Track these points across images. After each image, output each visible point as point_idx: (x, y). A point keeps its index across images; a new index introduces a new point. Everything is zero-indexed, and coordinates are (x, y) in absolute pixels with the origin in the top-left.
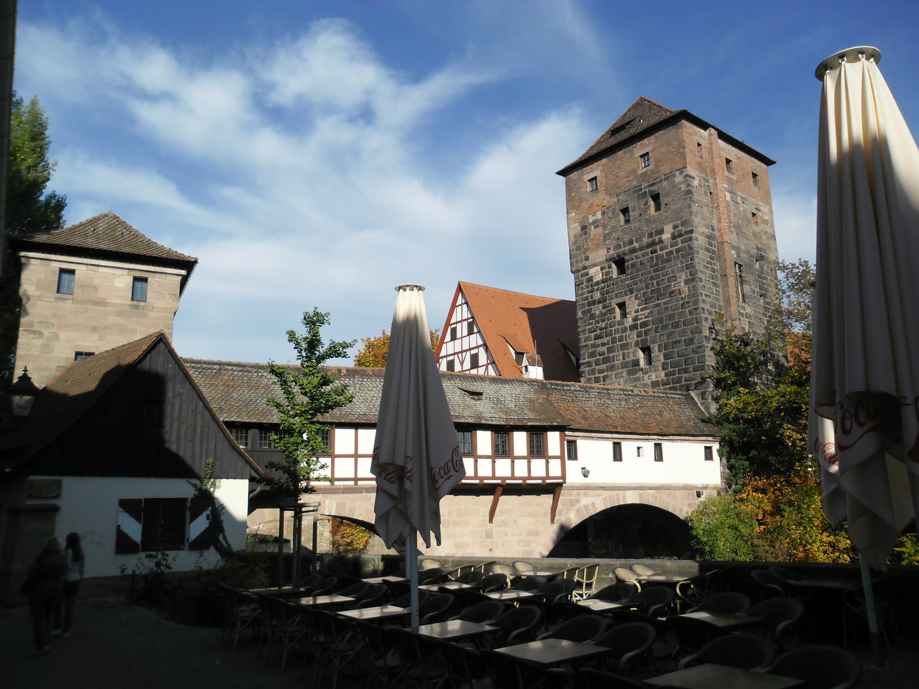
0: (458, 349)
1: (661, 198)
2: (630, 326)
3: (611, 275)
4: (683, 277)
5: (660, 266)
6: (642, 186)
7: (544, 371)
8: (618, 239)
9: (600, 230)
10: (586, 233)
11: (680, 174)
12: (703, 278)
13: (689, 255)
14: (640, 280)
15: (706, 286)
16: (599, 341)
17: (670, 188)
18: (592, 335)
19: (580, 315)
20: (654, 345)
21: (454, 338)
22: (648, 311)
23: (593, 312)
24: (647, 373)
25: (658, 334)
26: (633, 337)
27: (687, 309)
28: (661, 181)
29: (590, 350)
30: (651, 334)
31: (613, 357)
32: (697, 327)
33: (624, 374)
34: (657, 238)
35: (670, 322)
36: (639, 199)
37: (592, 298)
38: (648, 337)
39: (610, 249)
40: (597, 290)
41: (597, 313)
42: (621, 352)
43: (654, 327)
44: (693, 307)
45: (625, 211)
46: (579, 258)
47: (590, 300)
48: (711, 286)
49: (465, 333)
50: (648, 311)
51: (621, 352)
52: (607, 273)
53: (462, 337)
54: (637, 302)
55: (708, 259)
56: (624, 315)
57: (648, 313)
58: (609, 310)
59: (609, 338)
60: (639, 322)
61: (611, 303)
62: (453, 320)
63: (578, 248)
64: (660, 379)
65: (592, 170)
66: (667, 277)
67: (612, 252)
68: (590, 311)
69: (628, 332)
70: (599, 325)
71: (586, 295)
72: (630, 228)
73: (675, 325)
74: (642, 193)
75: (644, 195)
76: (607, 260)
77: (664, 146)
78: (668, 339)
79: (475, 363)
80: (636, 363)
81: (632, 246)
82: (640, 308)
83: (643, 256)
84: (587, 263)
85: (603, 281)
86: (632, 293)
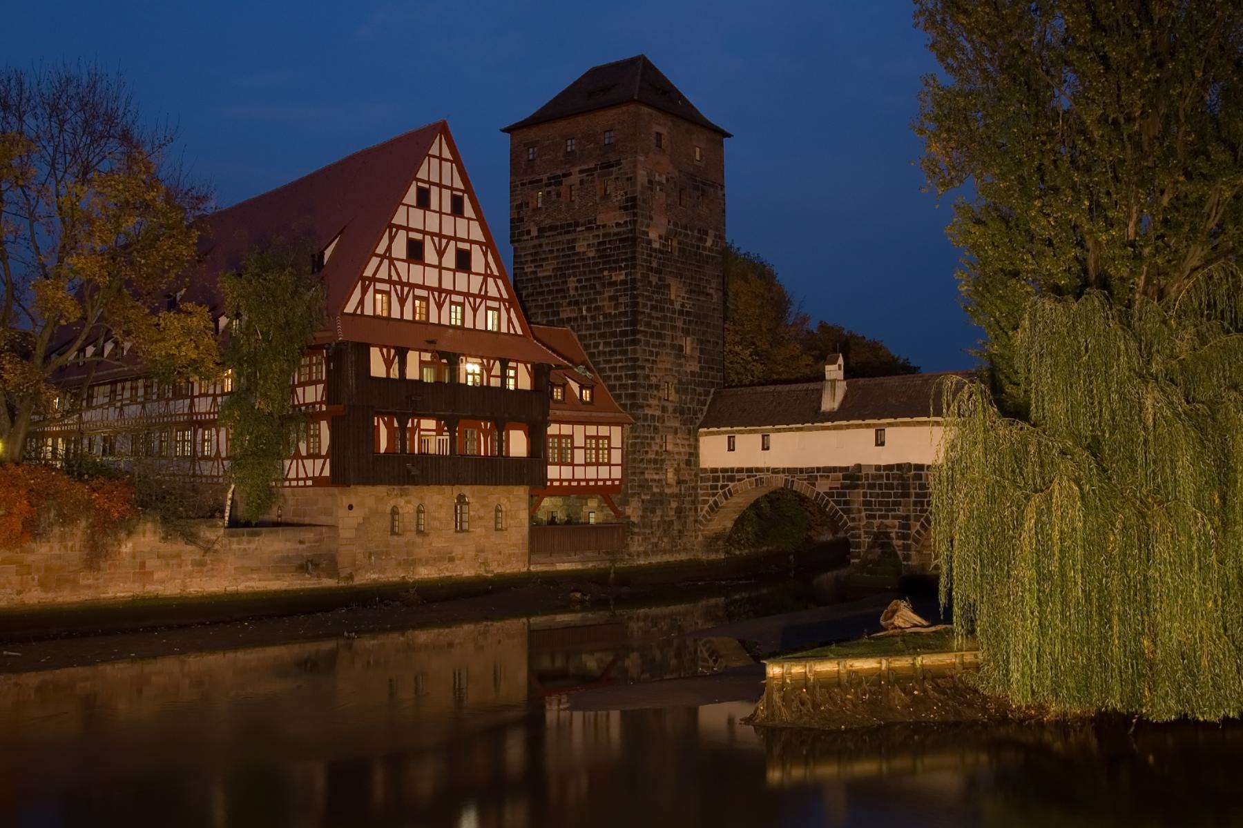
42: (670, 333)
60: (685, 309)
71: (645, 257)
79: (463, 261)
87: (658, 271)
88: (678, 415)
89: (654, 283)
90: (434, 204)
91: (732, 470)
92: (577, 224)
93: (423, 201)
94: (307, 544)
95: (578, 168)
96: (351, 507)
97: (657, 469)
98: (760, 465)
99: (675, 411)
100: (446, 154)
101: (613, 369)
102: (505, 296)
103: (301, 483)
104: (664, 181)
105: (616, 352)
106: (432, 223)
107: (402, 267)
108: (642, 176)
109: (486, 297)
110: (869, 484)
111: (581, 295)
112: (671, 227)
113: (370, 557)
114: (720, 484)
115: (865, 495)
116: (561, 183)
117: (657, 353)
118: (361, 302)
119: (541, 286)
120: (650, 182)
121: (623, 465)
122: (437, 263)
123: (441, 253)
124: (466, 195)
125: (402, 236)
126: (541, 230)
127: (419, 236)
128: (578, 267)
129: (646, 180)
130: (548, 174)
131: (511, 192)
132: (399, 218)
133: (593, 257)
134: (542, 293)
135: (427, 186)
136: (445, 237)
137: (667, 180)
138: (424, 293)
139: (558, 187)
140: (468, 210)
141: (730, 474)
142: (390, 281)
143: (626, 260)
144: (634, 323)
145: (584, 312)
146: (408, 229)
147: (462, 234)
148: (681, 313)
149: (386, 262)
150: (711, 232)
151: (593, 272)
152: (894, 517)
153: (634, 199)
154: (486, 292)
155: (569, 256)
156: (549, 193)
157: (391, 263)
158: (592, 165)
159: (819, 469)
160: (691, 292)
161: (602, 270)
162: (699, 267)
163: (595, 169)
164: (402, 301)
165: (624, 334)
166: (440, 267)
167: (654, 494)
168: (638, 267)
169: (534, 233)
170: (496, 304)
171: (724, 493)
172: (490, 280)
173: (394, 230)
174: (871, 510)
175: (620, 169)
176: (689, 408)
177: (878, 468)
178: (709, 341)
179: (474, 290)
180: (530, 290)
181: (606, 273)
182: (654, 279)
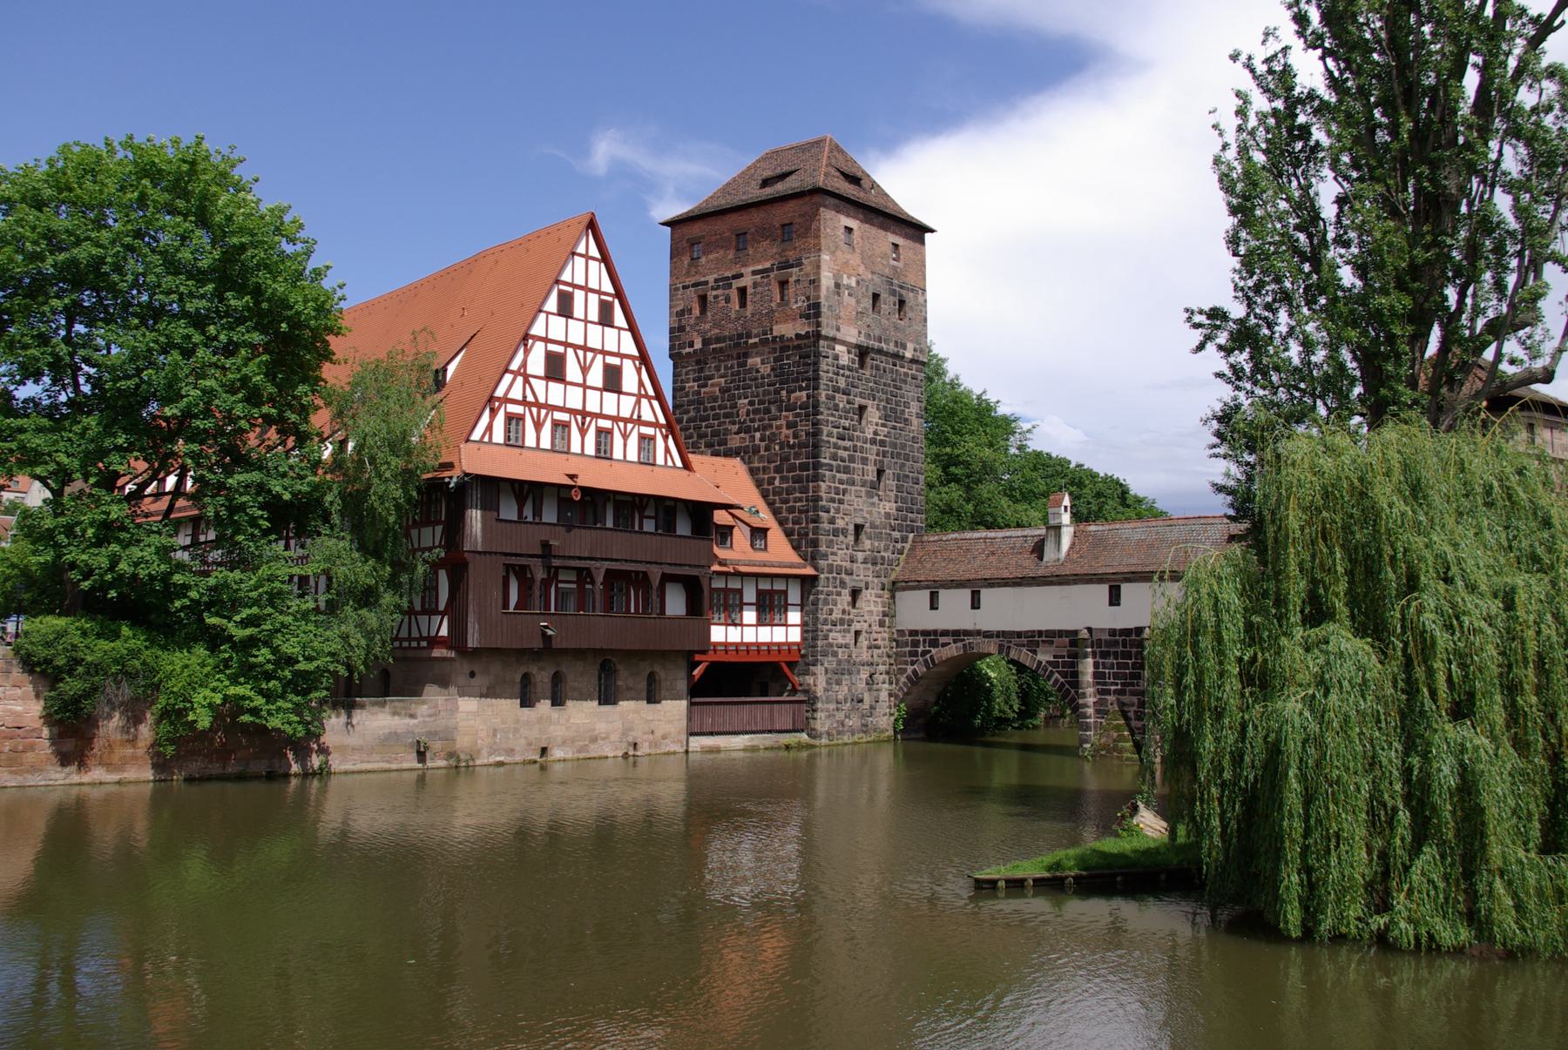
16: (840, 443)
19: (823, 398)
45: (876, 297)
67: (862, 338)
79: (612, 381)
84: (839, 336)
87: (844, 393)
88: (869, 565)
89: (841, 405)
90: (578, 311)
91: (935, 632)
92: (749, 336)
93: (565, 310)
94: (420, 719)
95: (751, 269)
96: (472, 675)
97: (844, 631)
98: (969, 626)
99: (865, 562)
100: (594, 252)
101: (791, 510)
102: (662, 420)
103: (414, 644)
104: (854, 284)
105: (795, 489)
106: (576, 334)
107: (539, 385)
108: (827, 280)
109: (639, 422)
110: (1101, 652)
111: (752, 421)
112: (862, 338)
113: (495, 735)
114: (920, 650)
115: (1096, 665)
116: (730, 286)
117: (845, 491)
118: (489, 428)
119: (705, 410)
120: (837, 286)
121: (804, 625)
122: (581, 381)
123: (585, 370)
124: (616, 302)
125: (539, 347)
126: (706, 342)
127: (560, 349)
128: (750, 387)
129: (832, 283)
130: (716, 276)
131: (671, 296)
132: (538, 329)
133: (769, 375)
134: (706, 419)
135: (570, 289)
136: (591, 350)
137: (858, 283)
138: (564, 417)
139: (727, 292)
140: (619, 318)
141: (933, 637)
142: (524, 402)
143: (808, 379)
144: (816, 456)
145: (757, 442)
146: (546, 340)
147: (611, 346)
148: (873, 442)
149: (520, 379)
150: (910, 346)
151: (769, 393)
152: (1133, 693)
153: (817, 306)
154: (639, 416)
155: (738, 373)
156: (716, 297)
157: (526, 381)
158: (768, 265)
159: (1040, 633)
160: (886, 418)
161: (777, 392)
162: (895, 387)
163: (770, 270)
164: (538, 426)
165: (804, 467)
166: (584, 386)
167: (839, 662)
168: (822, 387)
169: (698, 345)
170: (649, 431)
171: (926, 661)
172: (644, 402)
173: (530, 341)
174: (1105, 684)
175: (801, 270)
176: (883, 558)
177: (1113, 632)
178: (907, 476)
179: (626, 413)
180: (692, 414)
181: (784, 393)
182: (841, 401)
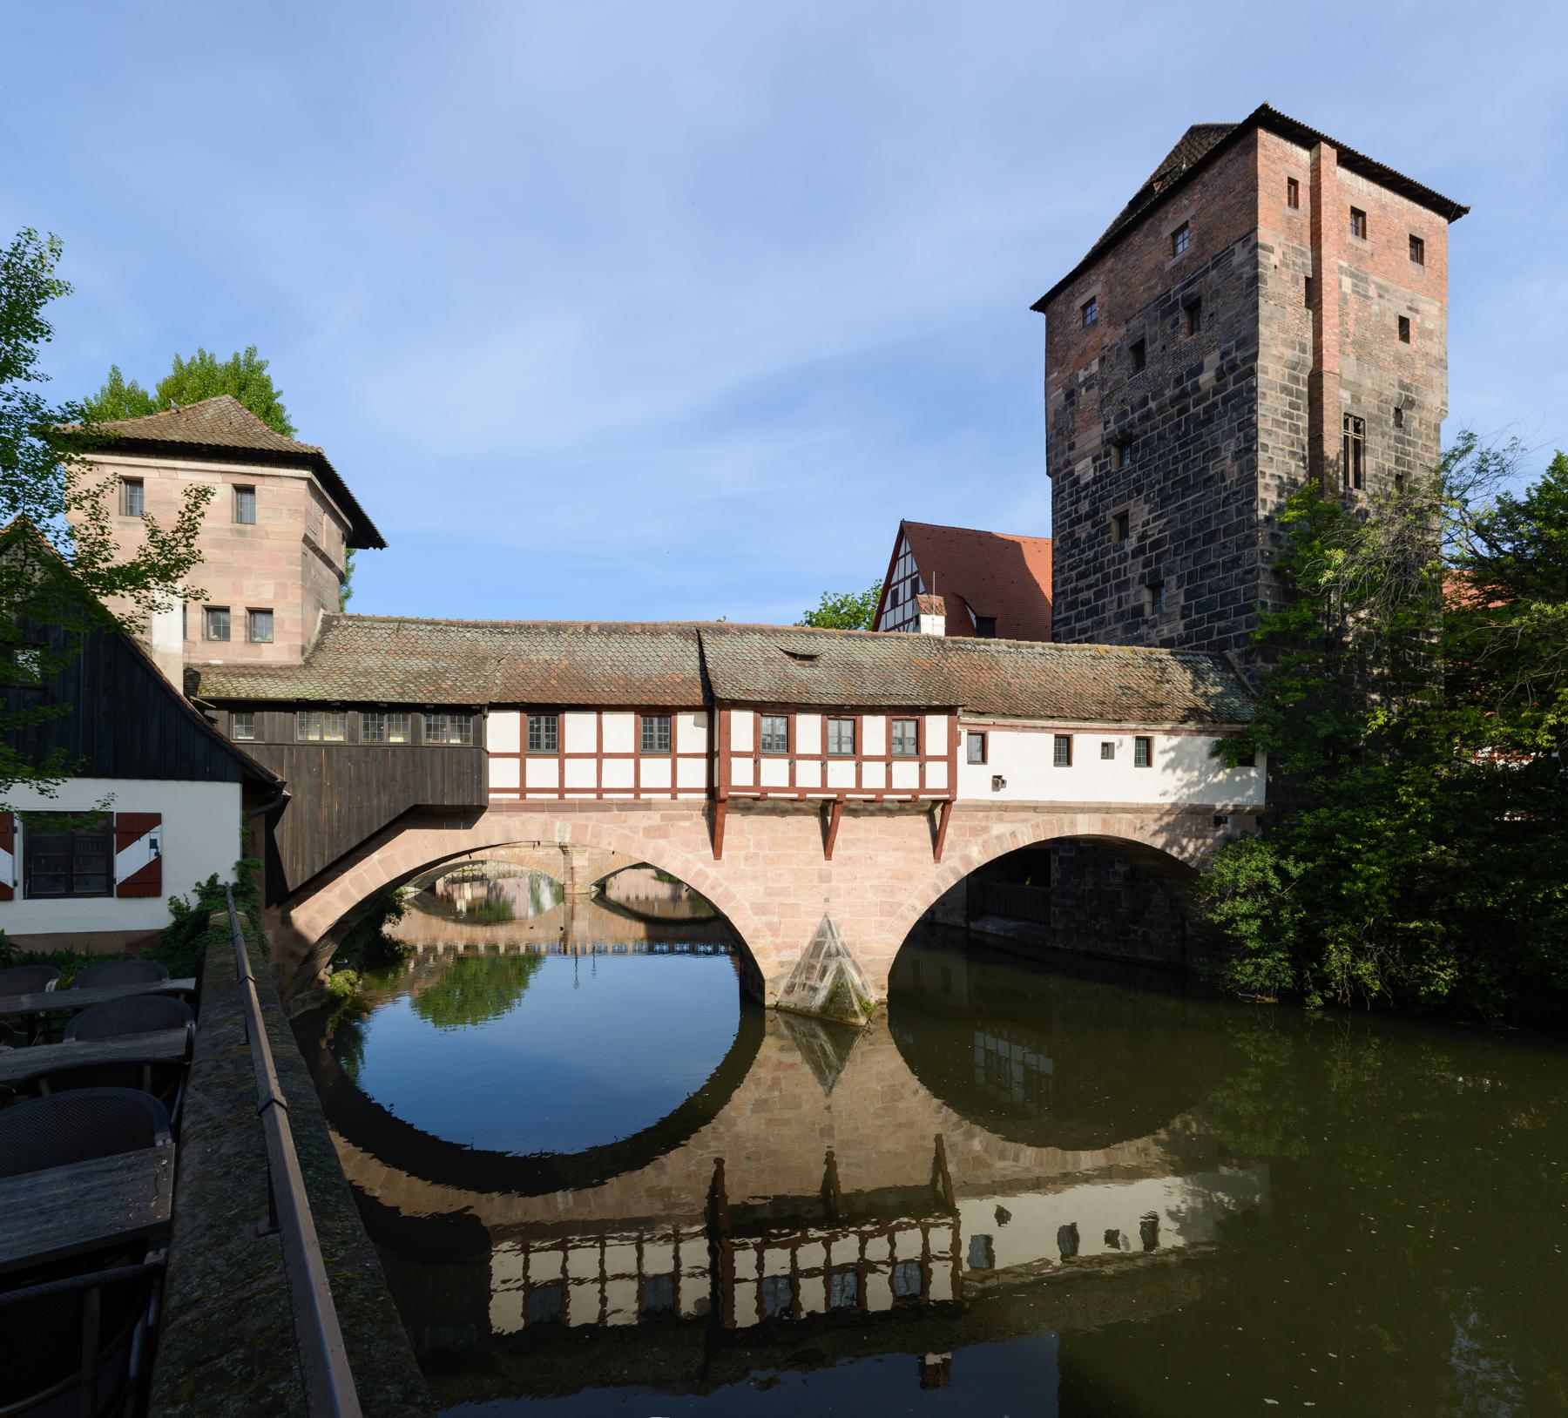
0: (899, 620)
1: (1204, 304)
2: (1133, 551)
3: (1109, 468)
4: (1229, 448)
5: (1192, 435)
6: (1172, 292)
7: (947, 622)
8: (1123, 401)
9: (1095, 390)
10: (1072, 404)
11: (1243, 247)
12: (1270, 444)
13: (1245, 404)
14: (1155, 468)
15: (1275, 458)
16: (1082, 583)
17: (1220, 281)
18: (1074, 573)
20: (1170, 578)
21: (895, 605)
22: (1165, 520)
23: (1077, 536)
24: (1154, 626)
25: (1178, 558)
26: (1135, 569)
27: (1234, 506)
28: (1207, 271)
29: (1069, 599)
30: (1166, 559)
31: (1104, 605)
32: (1249, 536)
33: (1119, 632)
34: (1189, 383)
35: (1201, 535)
36: (1163, 318)
37: (1076, 512)
38: (1161, 565)
39: (1109, 422)
40: (1085, 498)
41: (1083, 536)
43: (1172, 546)
44: (1244, 500)
46: (1060, 448)
47: (1074, 516)
48: (1287, 460)
49: (908, 596)
50: (1165, 520)
51: (1115, 597)
52: (1103, 466)
53: (905, 602)
54: (1147, 507)
55: (1287, 408)
56: (1124, 533)
57: (1165, 524)
58: (1102, 529)
59: (1099, 575)
60: (1148, 541)
61: (1104, 516)
62: (894, 580)
63: (1060, 432)
64: (1175, 635)
65: (1089, 286)
66: (1202, 454)
68: (1072, 534)
69: (1130, 561)
70: (1083, 556)
71: (1068, 509)
72: (1145, 377)
73: (1211, 537)
74: (1170, 306)
75: (1175, 305)
76: (1103, 442)
77: (1217, 199)
78: (1194, 565)
80: (1138, 611)
81: (1146, 409)
82: (1151, 516)
83: (1164, 423)
85: (1095, 481)
86: (1139, 493)
